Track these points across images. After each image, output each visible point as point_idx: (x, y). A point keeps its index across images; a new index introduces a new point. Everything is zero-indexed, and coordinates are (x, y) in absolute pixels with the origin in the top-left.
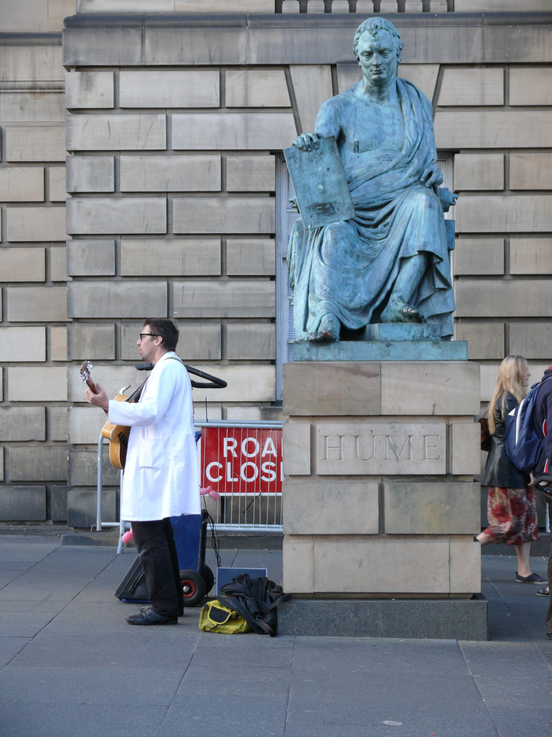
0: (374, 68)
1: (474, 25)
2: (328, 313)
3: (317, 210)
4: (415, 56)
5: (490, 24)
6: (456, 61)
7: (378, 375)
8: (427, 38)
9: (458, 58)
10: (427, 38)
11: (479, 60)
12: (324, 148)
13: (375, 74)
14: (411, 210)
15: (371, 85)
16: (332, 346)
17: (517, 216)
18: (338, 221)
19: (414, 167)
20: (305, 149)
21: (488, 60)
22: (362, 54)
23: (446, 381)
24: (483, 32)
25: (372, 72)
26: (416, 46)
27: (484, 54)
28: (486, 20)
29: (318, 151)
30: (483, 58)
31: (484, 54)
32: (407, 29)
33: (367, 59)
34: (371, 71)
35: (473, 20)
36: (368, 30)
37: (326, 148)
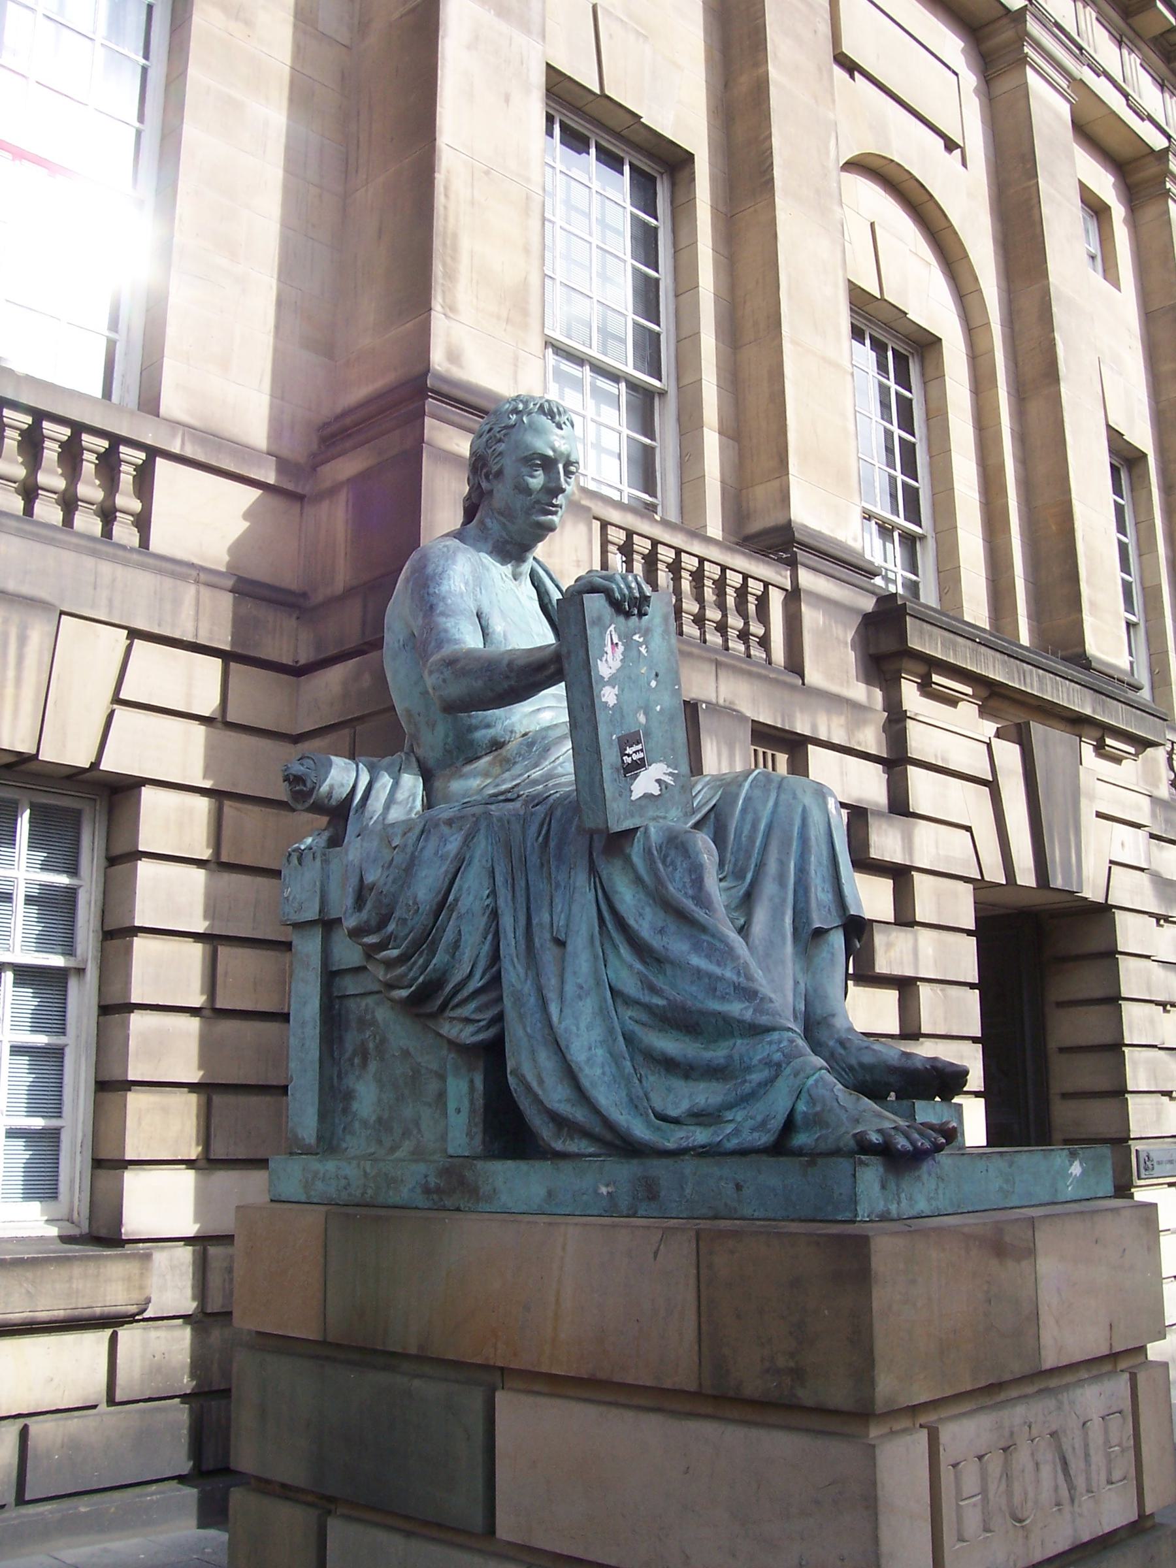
1: (183, 578)
4: (93, 606)
5: (208, 585)
6: (156, 630)
7: (1030, 1252)
8: (114, 580)
10: (114, 580)
11: (189, 637)
16: (926, 1167)
17: (230, 908)
18: (665, 818)
21: (202, 641)
23: (1122, 1257)
24: (198, 592)
25: (537, 506)
26: (95, 588)
28: (203, 577)
32: (84, 557)
35: (184, 570)
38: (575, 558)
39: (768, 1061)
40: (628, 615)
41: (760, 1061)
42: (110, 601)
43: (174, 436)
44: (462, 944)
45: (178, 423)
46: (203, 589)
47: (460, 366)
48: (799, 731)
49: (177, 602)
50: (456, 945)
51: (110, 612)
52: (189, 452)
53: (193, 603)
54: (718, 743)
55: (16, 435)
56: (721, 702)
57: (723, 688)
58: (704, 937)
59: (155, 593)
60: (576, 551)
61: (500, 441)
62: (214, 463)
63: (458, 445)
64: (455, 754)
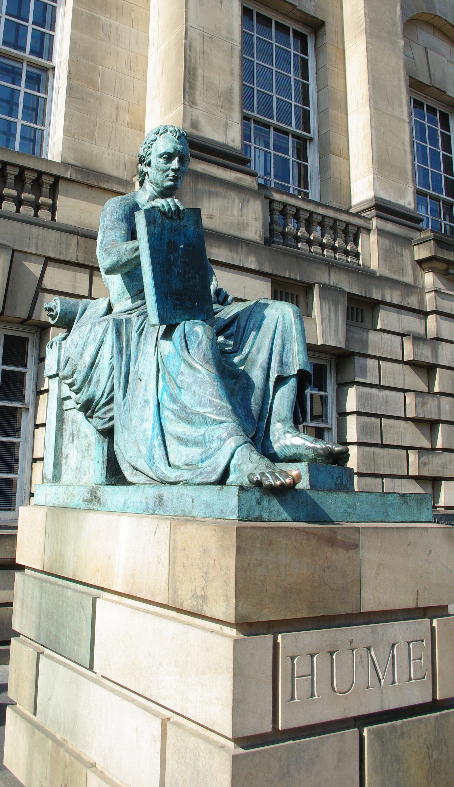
0: (172, 174)
2: (246, 443)
3: (174, 299)
4: (28, 247)
6: (58, 257)
8: (38, 235)
9: (60, 255)
10: (38, 235)
11: (74, 260)
12: (188, 220)
13: (170, 180)
14: (276, 320)
15: (157, 195)
19: (214, 284)
20: (170, 215)
21: (80, 261)
22: (161, 156)
26: (30, 239)
27: (77, 256)
29: (182, 223)
30: (77, 259)
31: (77, 256)
33: (165, 162)
34: (167, 176)
36: (171, 132)
37: (191, 222)
38: (255, 217)
39: (220, 438)
40: (171, 218)
41: (217, 438)
42: (37, 244)
43: (67, 170)
44: (101, 381)
45: (70, 164)
46: (80, 238)
47: (198, 130)
48: (374, 298)
49: (68, 245)
50: (98, 382)
51: (37, 250)
52: (74, 177)
53: (76, 244)
54: (329, 304)
55: (13, 177)
56: (332, 284)
57: (332, 277)
58: (200, 376)
59: (58, 241)
60: (255, 213)
61: (149, 148)
62: (86, 181)
63: (195, 166)
64: (122, 296)
